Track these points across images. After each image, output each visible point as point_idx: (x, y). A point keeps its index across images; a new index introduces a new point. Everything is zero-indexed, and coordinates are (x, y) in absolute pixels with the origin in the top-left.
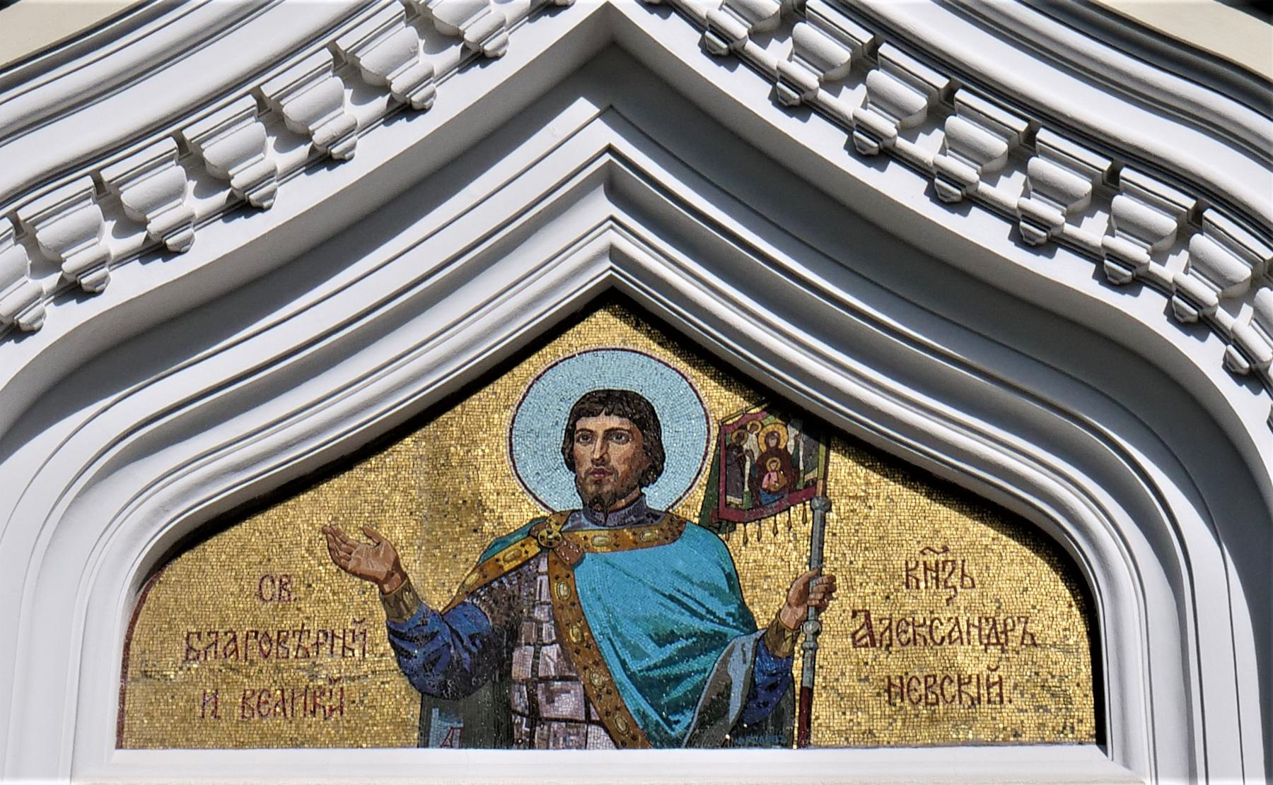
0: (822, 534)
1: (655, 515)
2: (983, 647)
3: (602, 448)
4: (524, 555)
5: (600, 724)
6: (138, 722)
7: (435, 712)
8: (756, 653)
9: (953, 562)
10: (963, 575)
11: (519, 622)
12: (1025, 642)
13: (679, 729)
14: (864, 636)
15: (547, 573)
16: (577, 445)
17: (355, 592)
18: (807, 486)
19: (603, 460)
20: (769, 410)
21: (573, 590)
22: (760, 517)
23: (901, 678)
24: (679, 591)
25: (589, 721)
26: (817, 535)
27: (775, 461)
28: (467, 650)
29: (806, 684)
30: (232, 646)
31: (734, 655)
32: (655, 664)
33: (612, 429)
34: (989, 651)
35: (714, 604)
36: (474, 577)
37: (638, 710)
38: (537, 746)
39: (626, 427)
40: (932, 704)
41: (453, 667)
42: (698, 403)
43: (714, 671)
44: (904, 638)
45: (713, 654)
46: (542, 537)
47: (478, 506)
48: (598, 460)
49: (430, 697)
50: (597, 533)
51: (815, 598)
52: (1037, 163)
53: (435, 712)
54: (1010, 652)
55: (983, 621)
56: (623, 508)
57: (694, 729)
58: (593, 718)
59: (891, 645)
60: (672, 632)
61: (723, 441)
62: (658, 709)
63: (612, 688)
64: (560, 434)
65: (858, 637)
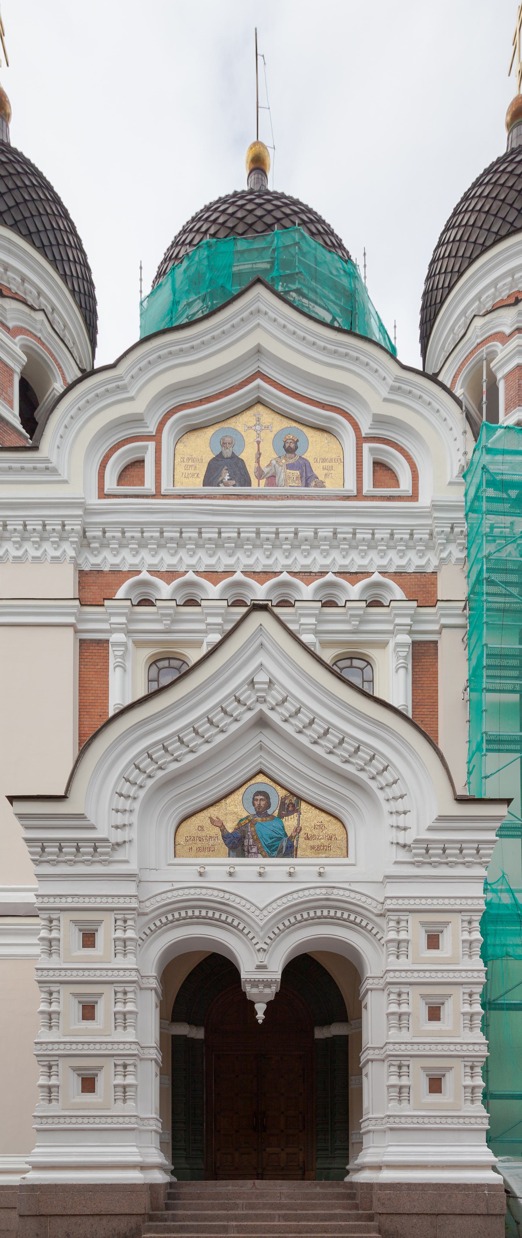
1: (269, 815)
6: (177, 852)
19: (260, 804)
35: (280, 832)
41: (234, 843)
51: (298, 831)
62: (271, 851)
63: (262, 847)
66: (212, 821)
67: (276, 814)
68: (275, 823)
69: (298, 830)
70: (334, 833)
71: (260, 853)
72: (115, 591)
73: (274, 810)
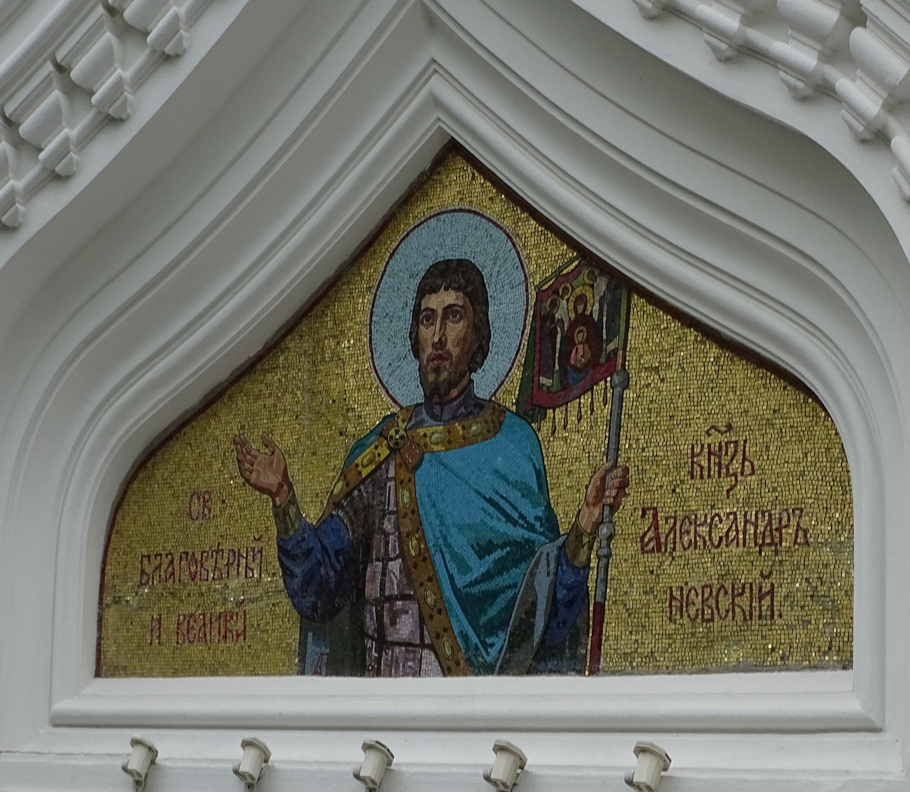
1: (480, 404)
2: (757, 549)
3: (440, 330)
4: (377, 459)
5: (431, 647)
8: (558, 563)
9: (736, 442)
10: (744, 459)
12: (799, 540)
14: (650, 540)
15: (394, 478)
16: (422, 327)
19: (441, 344)
21: (413, 496)
22: (566, 400)
23: (682, 589)
24: (497, 493)
25: (423, 645)
26: (615, 418)
27: (581, 331)
29: (599, 599)
31: (540, 566)
32: (476, 579)
33: (450, 306)
34: (763, 554)
36: (340, 485)
37: (462, 631)
38: (382, 673)
39: (461, 303)
40: (708, 621)
42: (520, 267)
43: (523, 585)
45: (523, 566)
46: (391, 437)
48: (437, 343)
50: (434, 428)
51: (611, 493)
53: (310, 634)
54: (784, 553)
55: (760, 516)
56: (456, 398)
57: (505, 653)
58: (426, 642)
59: (674, 549)
60: (491, 541)
61: (539, 311)
65: (646, 540)
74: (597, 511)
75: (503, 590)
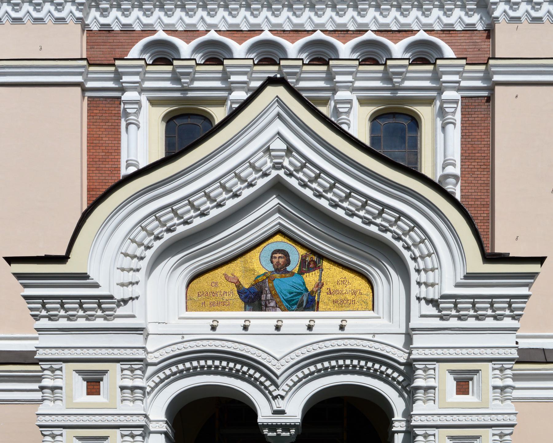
0: (321, 275)
1: (288, 272)
5: (279, 307)
6: (189, 307)
7: (247, 305)
8: (308, 295)
11: (263, 290)
13: (294, 308)
17: (230, 285)
18: (318, 267)
19: (278, 262)
20: (311, 253)
28: (253, 295)
30: (207, 294)
41: (250, 298)
44: (337, 293)
45: (300, 296)
47: (254, 270)
49: (246, 303)
51: (320, 286)
52: (367, 207)
53: (247, 305)
62: (289, 305)
63: (281, 302)
64: (270, 257)
66: (226, 277)
67: (296, 270)
68: (295, 279)
69: (320, 285)
70: (359, 288)
71: (279, 306)
72: (128, 50)
73: (294, 266)
74: (317, 289)
75: (295, 299)
